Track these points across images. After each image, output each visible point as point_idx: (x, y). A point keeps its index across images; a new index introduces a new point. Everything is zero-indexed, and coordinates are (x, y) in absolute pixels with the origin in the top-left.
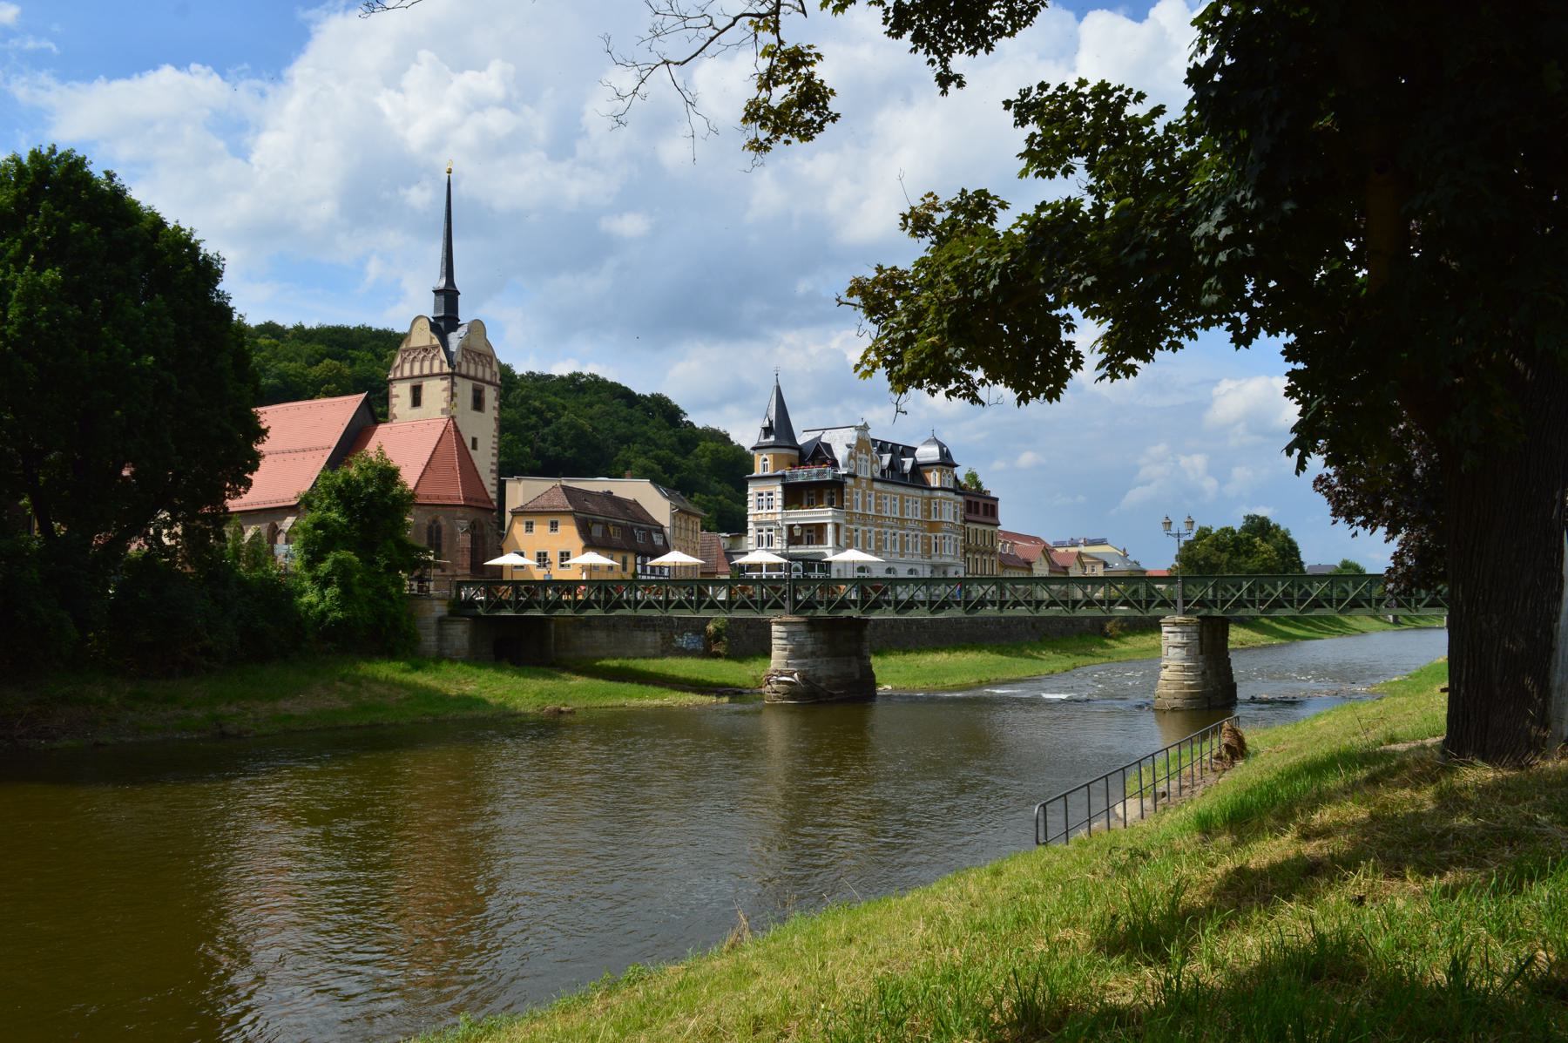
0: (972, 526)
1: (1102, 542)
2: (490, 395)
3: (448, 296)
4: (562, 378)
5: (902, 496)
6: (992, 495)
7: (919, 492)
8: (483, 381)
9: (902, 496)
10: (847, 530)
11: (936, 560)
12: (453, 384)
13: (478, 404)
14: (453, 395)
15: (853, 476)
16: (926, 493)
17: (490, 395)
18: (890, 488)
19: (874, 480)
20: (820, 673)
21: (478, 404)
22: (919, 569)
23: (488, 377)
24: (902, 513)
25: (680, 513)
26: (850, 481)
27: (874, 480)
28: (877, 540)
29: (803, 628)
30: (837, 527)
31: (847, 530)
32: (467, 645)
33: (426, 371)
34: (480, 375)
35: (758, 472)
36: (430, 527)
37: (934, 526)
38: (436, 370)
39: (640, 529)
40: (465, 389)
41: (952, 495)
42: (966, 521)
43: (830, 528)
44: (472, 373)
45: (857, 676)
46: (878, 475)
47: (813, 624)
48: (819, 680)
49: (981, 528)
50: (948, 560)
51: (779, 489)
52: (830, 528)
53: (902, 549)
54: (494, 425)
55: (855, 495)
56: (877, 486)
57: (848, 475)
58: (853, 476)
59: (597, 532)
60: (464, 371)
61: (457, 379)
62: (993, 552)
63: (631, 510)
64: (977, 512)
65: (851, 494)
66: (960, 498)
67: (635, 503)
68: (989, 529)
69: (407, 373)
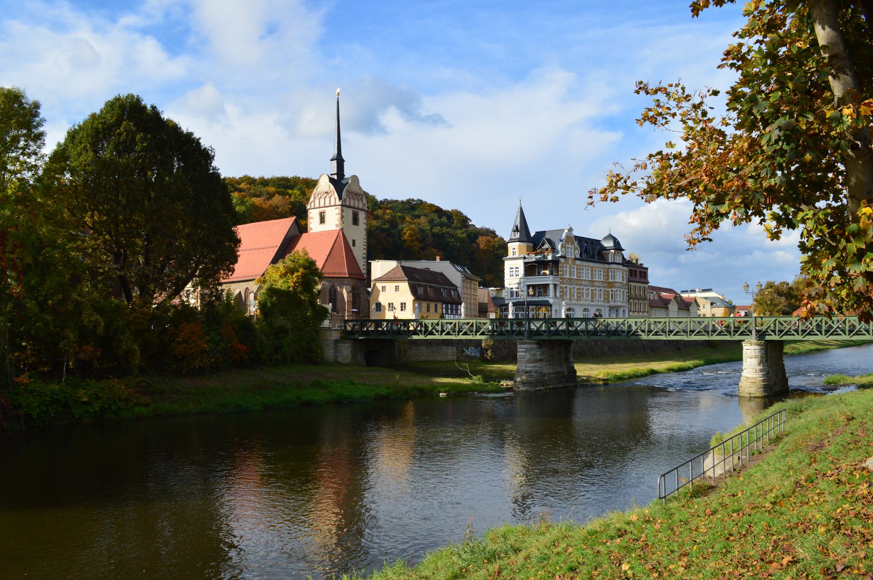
0: (633, 284)
1: (710, 290)
2: (362, 216)
3: (340, 161)
4: (403, 202)
5: (592, 268)
6: (644, 266)
7: (602, 265)
8: (358, 208)
9: (592, 268)
10: (561, 288)
11: (612, 304)
12: (342, 211)
13: (355, 221)
14: (342, 217)
15: (564, 257)
16: (606, 266)
17: (362, 216)
18: (585, 263)
19: (576, 259)
20: (545, 371)
21: (355, 221)
22: (602, 309)
23: (361, 207)
24: (592, 277)
25: (466, 278)
26: (562, 260)
27: (576, 259)
28: (578, 293)
29: (535, 346)
30: (555, 286)
31: (561, 288)
32: (350, 355)
33: (327, 204)
34: (356, 205)
35: (510, 255)
36: (330, 290)
37: (611, 285)
38: (333, 203)
39: (444, 289)
40: (349, 213)
41: (621, 267)
42: (629, 281)
43: (551, 287)
44: (352, 205)
45: (566, 373)
46: (578, 256)
47: (541, 344)
48: (545, 375)
49: (638, 285)
50: (619, 304)
51: (522, 265)
52: (551, 287)
53: (592, 298)
54: (364, 233)
55: (566, 270)
56: (578, 262)
57: (561, 257)
59: (421, 291)
60: (348, 204)
61: (344, 208)
62: (645, 299)
63: (440, 278)
64: (636, 276)
65: (563, 267)
66: (626, 268)
67: (442, 274)
68: (642, 285)
69: (317, 205)
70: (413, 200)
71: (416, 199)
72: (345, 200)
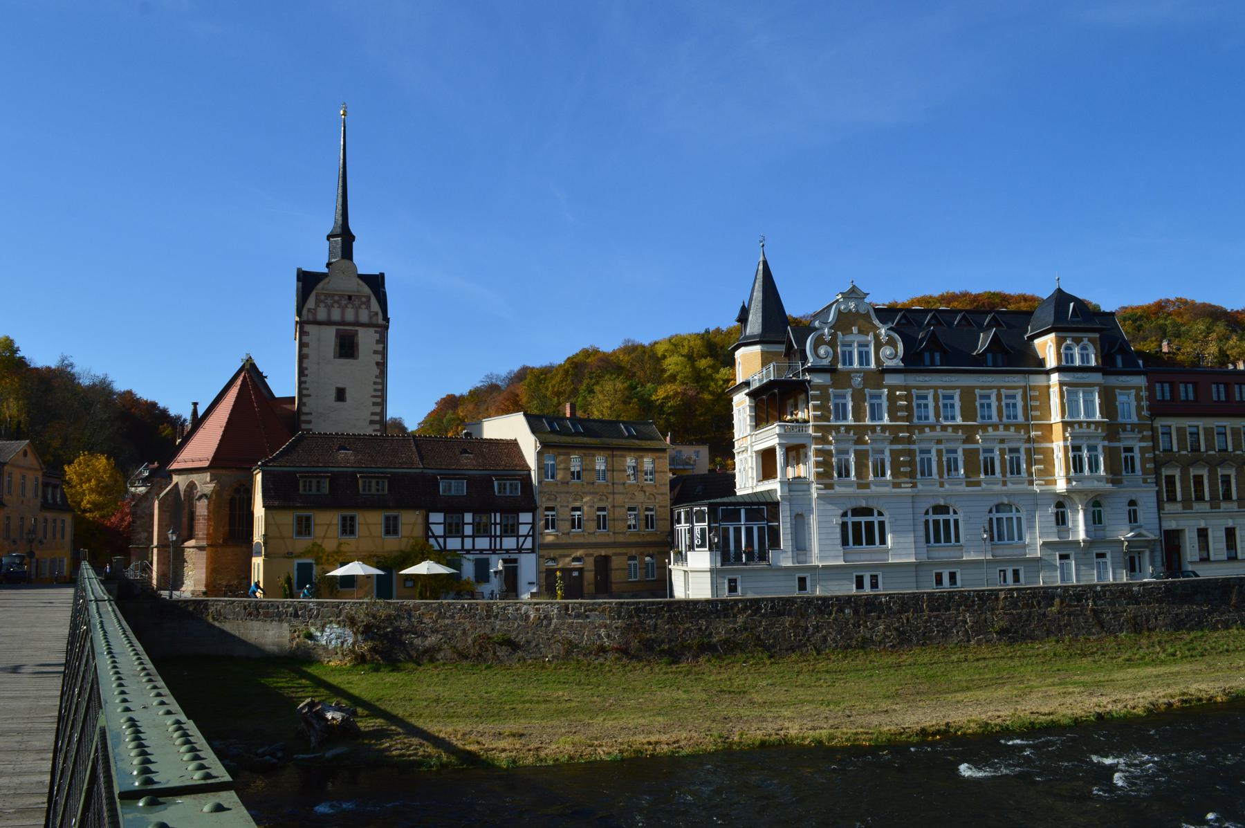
0: (1160, 423)
3: (344, 238)
9: (967, 394)
15: (831, 370)
23: (364, 316)
25: (546, 447)
34: (350, 315)
40: (329, 336)
41: (1097, 378)
44: (336, 315)
46: (897, 363)
56: (890, 380)
57: (811, 370)
58: (831, 370)
60: (322, 314)
61: (308, 328)
70: (1168, 301)
71: (1172, 298)
72: (313, 312)
